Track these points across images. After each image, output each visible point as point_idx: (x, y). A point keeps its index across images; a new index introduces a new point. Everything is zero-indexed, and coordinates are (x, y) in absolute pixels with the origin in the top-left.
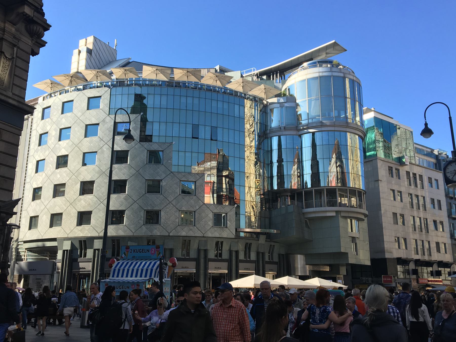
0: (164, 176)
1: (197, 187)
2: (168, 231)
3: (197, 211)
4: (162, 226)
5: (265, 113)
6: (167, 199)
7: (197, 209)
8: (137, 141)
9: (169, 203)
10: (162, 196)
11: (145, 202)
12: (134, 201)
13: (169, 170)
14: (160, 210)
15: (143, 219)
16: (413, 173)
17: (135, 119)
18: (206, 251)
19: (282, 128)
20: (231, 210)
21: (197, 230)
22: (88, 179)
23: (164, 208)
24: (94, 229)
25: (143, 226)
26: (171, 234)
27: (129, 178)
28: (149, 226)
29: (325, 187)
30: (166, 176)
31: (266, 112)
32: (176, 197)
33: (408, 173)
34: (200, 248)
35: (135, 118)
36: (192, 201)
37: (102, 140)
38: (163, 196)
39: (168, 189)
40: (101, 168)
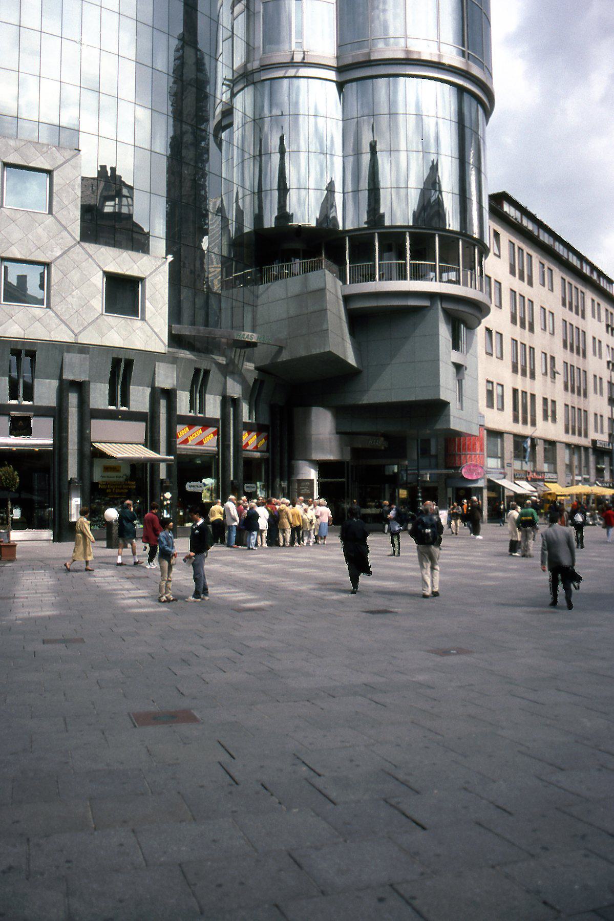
1: (55, 189)
7: (58, 257)
18: (81, 388)
21: (57, 321)
29: (408, 227)
31: (252, 9)
34: (64, 377)
36: (40, 230)
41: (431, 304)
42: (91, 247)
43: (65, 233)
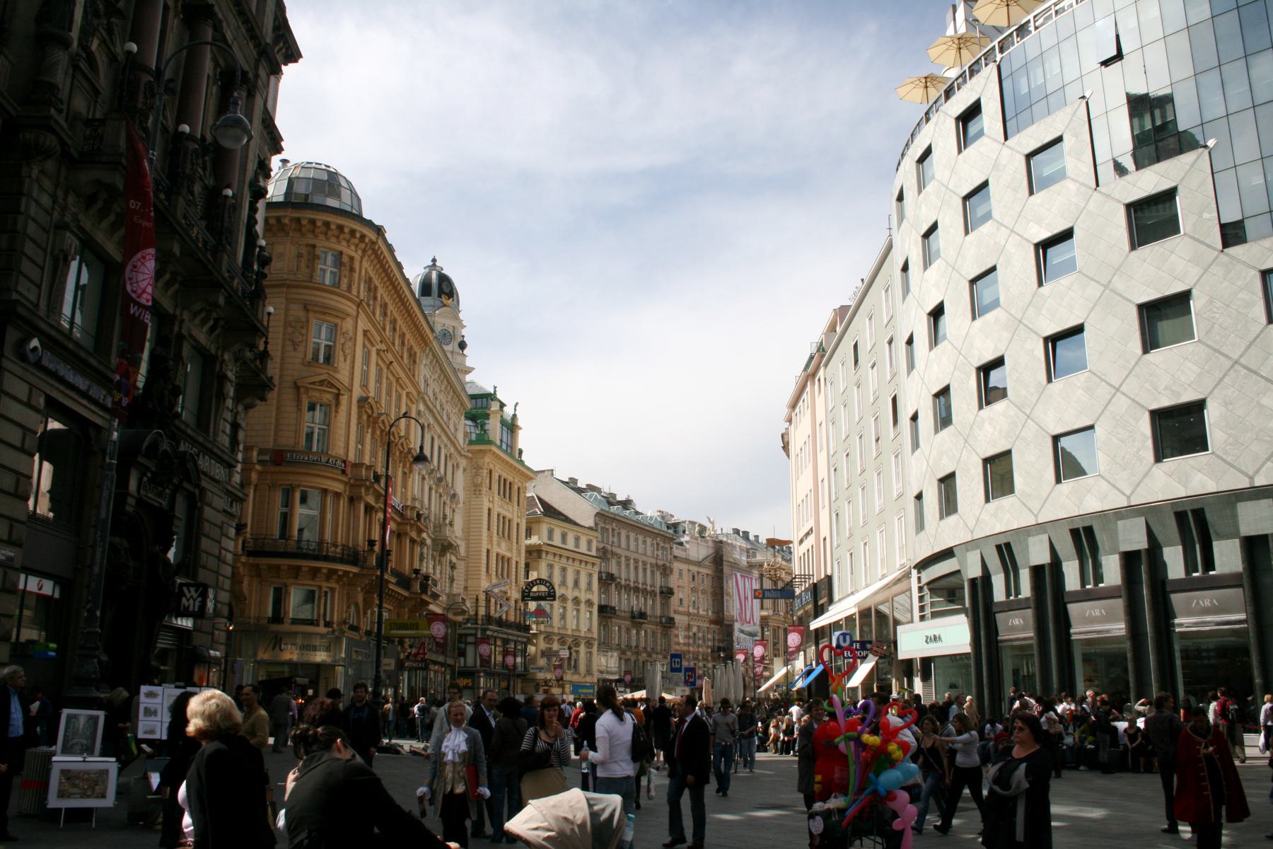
0: (1194, 272)
2: (1243, 468)
4: (1218, 457)
8: (1090, 188)
9: (1232, 367)
10: (1202, 347)
11: (1147, 385)
12: (1114, 387)
13: (1209, 246)
17: (1071, 119)
22: (989, 357)
24: (1024, 504)
26: (1260, 481)
27: (1088, 317)
28: (1172, 463)
30: (1203, 274)
35: (1070, 117)
37: (1002, 224)
38: (1208, 346)
39: (1217, 316)
40: (1013, 311)
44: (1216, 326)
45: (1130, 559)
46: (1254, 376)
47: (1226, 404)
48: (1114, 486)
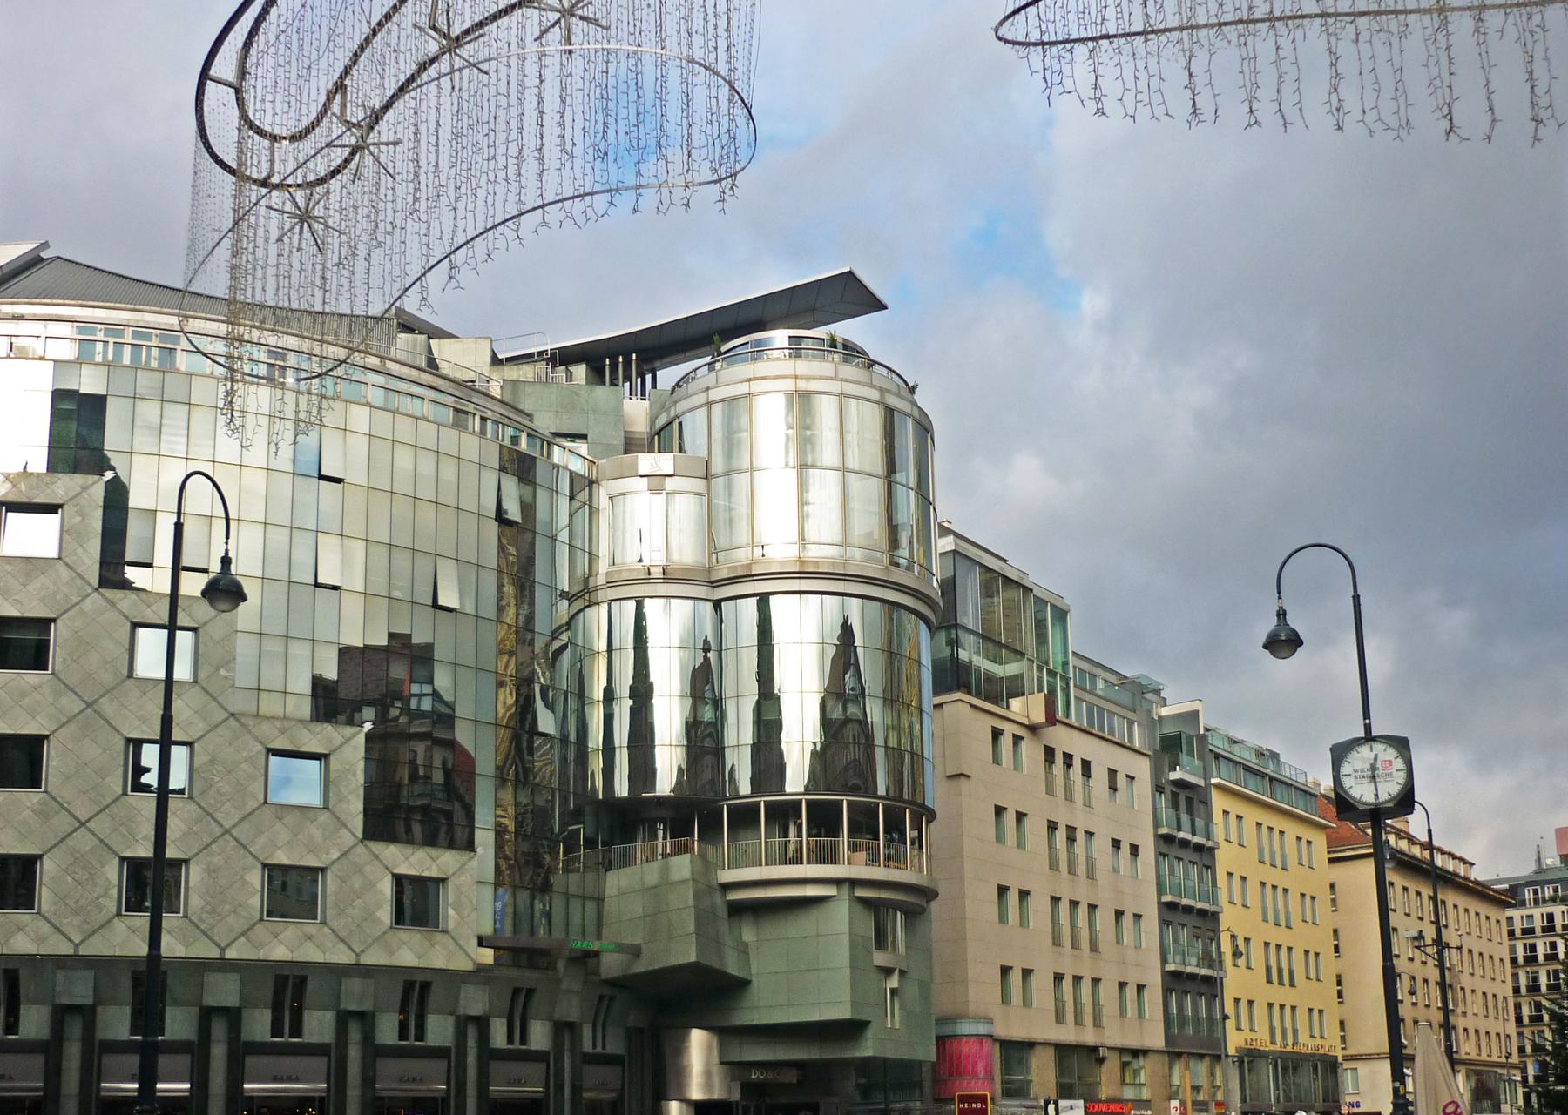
3: (334, 868)
5: (590, 506)
6: (216, 820)
7: (334, 862)
9: (221, 835)
10: (193, 806)
14: (186, 861)
15: (114, 892)
16: (1064, 754)
19: (657, 572)
20: (463, 866)
23: (201, 851)
25: (116, 920)
31: (595, 505)
32: (249, 814)
33: (1049, 752)
39: (216, 779)
41: (838, 891)
42: (376, 847)
43: (344, 832)
44: (213, 790)
45: (61, 1014)
46: (242, 851)
47: (211, 871)
48: (59, 930)
